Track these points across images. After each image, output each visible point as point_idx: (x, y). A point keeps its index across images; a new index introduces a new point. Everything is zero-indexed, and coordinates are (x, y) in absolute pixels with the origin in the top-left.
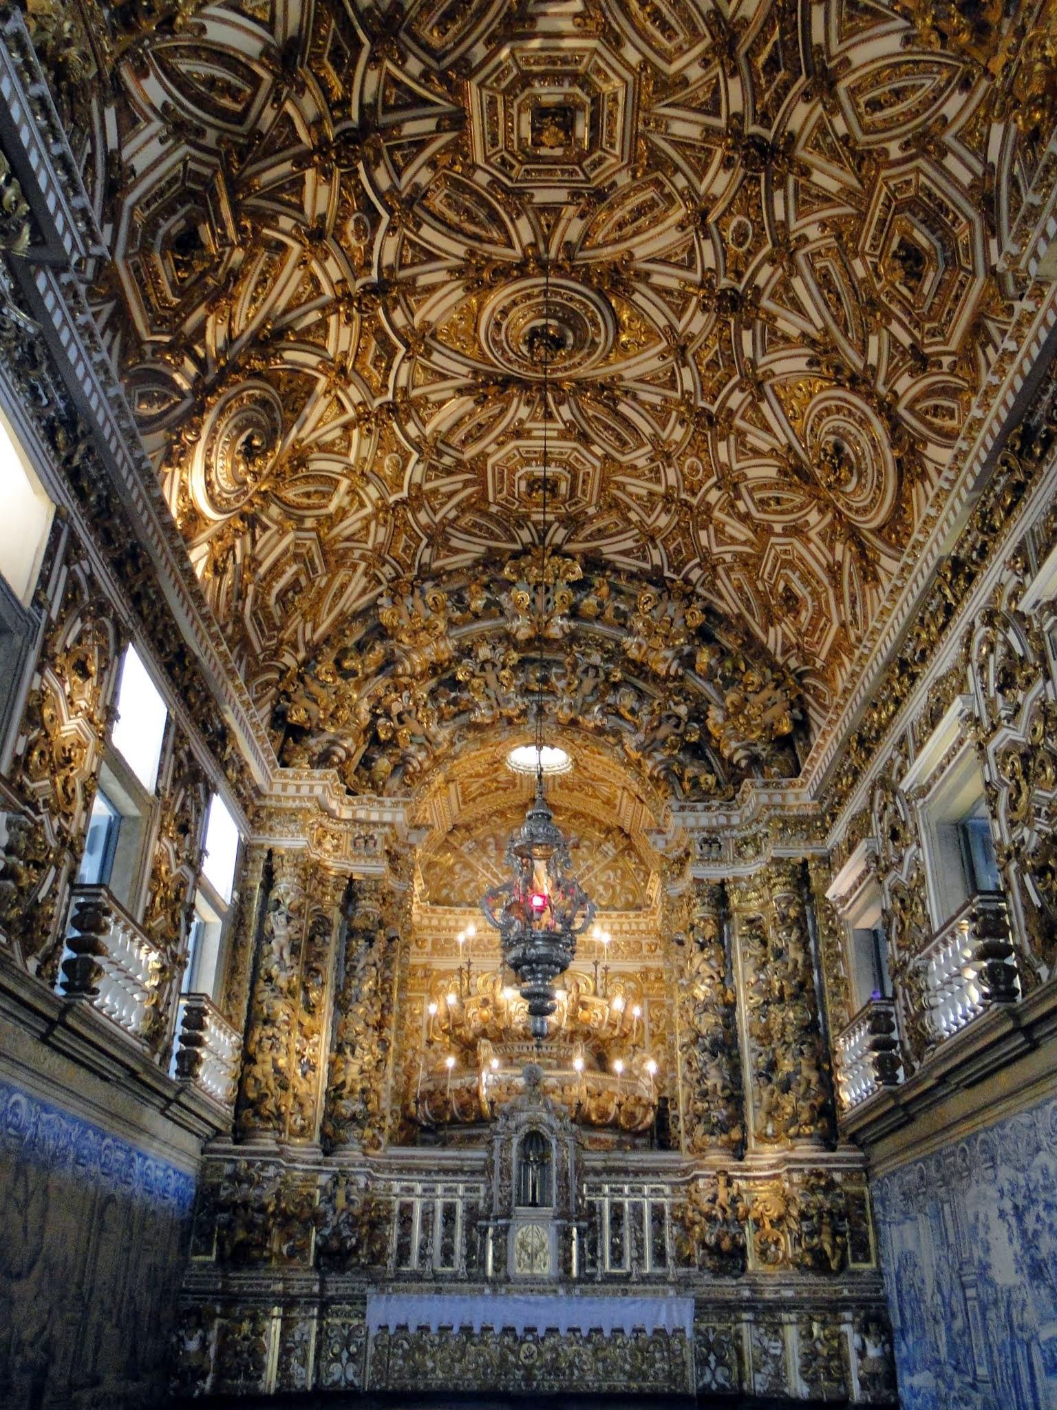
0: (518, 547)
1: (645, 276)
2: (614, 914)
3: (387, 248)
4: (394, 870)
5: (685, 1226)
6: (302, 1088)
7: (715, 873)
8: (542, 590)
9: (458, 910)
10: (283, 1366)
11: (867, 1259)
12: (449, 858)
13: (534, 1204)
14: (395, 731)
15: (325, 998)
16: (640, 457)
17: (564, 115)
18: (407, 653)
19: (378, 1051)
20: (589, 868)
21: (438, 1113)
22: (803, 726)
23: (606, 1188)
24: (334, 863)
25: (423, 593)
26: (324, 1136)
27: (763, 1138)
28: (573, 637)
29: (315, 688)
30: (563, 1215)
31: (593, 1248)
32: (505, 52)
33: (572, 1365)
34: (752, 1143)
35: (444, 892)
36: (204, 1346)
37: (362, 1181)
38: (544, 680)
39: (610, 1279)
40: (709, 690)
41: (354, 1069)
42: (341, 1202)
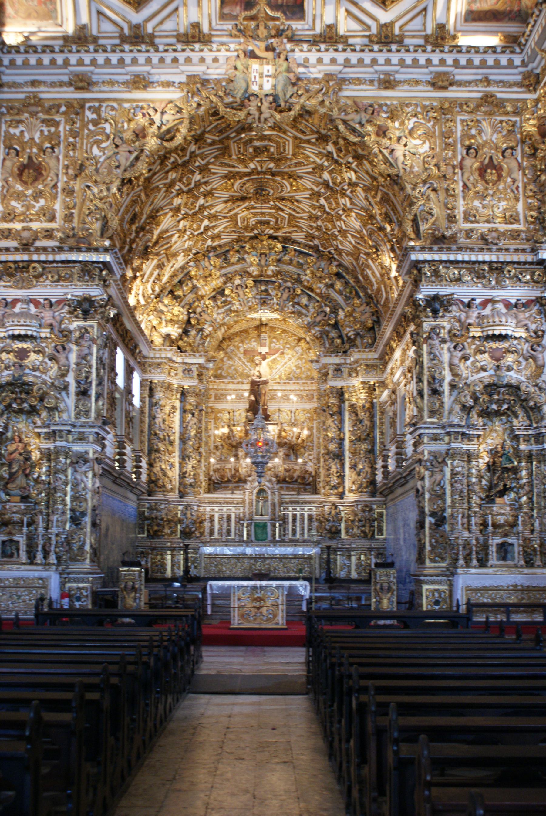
0: (252, 234)
4: (201, 380)
5: (321, 522)
6: (170, 474)
7: (338, 384)
8: (263, 256)
10: (173, 570)
11: (382, 535)
12: (221, 354)
13: (262, 515)
16: (305, 215)
19: (198, 458)
21: (222, 477)
22: (378, 322)
23: (290, 509)
24: (175, 382)
25: (209, 259)
27: (351, 491)
28: (277, 273)
31: (285, 530)
32: (243, 135)
33: (275, 569)
34: (347, 492)
35: (219, 371)
37: (195, 507)
38: (266, 291)
39: (291, 541)
40: (340, 299)
42: (189, 516)
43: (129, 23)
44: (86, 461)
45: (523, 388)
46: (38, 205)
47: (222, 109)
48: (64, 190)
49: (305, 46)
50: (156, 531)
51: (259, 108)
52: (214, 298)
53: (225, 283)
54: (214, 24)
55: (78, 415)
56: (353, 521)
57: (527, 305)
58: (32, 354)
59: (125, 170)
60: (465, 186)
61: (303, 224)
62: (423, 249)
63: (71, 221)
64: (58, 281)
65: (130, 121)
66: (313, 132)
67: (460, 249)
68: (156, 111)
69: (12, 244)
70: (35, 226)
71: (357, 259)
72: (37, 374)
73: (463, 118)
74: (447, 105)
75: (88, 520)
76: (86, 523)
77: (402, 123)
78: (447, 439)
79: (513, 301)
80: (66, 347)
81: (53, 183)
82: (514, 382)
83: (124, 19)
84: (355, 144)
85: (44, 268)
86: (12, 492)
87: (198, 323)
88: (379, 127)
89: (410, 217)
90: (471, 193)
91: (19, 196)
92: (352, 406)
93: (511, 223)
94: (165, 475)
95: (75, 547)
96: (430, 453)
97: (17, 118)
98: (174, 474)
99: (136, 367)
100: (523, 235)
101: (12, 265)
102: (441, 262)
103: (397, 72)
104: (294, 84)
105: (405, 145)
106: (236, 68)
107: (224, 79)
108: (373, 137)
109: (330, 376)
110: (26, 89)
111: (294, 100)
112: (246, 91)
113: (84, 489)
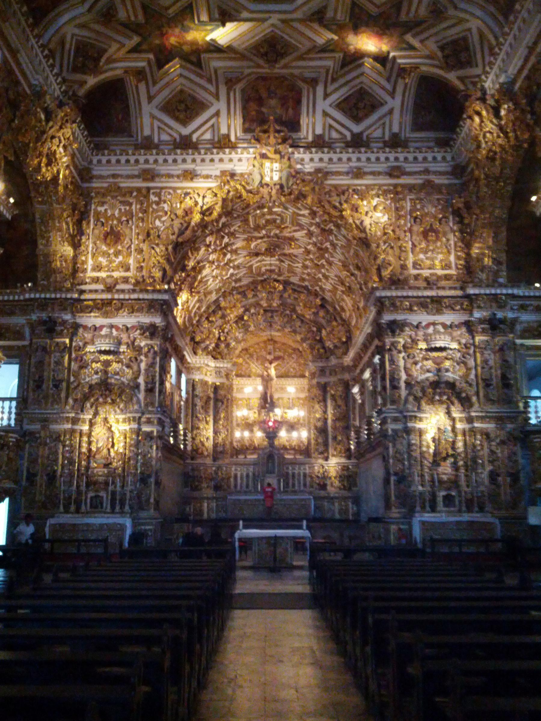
0: (262, 278)
1: (297, 240)
2: (296, 379)
3: (226, 240)
6: (206, 444)
7: (323, 380)
9: (244, 379)
10: (208, 513)
12: (240, 360)
14: (226, 337)
15: (211, 419)
16: (300, 265)
17: (275, 221)
18: (229, 314)
20: (288, 363)
25: (233, 295)
26: (213, 457)
27: (333, 455)
29: (202, 329)
30: (278, 476)
34: (330, 457)
36: (190, 508)
37: (224, 468)
38: (272, 317)
40: (323, 322)
41: (220, 439)
42: (220, 474)
43: (180, 135)
44: (152, 438)
45: (458, 384)
46: (117, 261)
47: (244, 194)
48: (136, 250)
49: (302, 150)
50: (197, 486)
51: (270, 193)
52: (236, 322)
53: (244, 312)
54: (238, 135)
55: (146, 405)
56: (335, 478)
57: (458, 326)
58: (114, 363)
59: (179, 236)
60: (414, 245)
61: (298, 270)
62: (384, 289)
63: (142, 271)
64: (133, 312)
65: (181, 203)
66: (306, 208)
67: (410, 288)
68: (199, 195)
69: (100, 287)
70: (116, 274)
71: (335, 295)
72: (118, 377)
73: (411, 197)
74: (399, 189)
75: (152, 480)
76: (151, 483)
77: (369, 202)
78: (404, 420)
79: (448, 323)
80: (138, 358)
81: (128, 245)
82: (451, 380)
83: (177, 131)
84: (336, 217)
85: (122, 304)
86: (98, 461)
87: (226, 340)
88: (353, 205)
89: (376, 267)
90: (418, 249)
91: (105, 254)
92: (333, 396)
93: (446, 269)
94: (203, 445)
95: (144, 499)
96: (393, 430)
97: (103, 200)
98: (209, 444)
99: (184, 370)
100: (455, 277)
101: (99, 301)
102: (397, 297)
103: (365, 167)
104: (294, 177)
105: (371, 217)
106: (254, 166)
107: (246, 174)
108: (349, 212)
109: (316, 376)
110: (108, 180)
111: (294, 187)
112: (261, 182)
113: (150, 458)
